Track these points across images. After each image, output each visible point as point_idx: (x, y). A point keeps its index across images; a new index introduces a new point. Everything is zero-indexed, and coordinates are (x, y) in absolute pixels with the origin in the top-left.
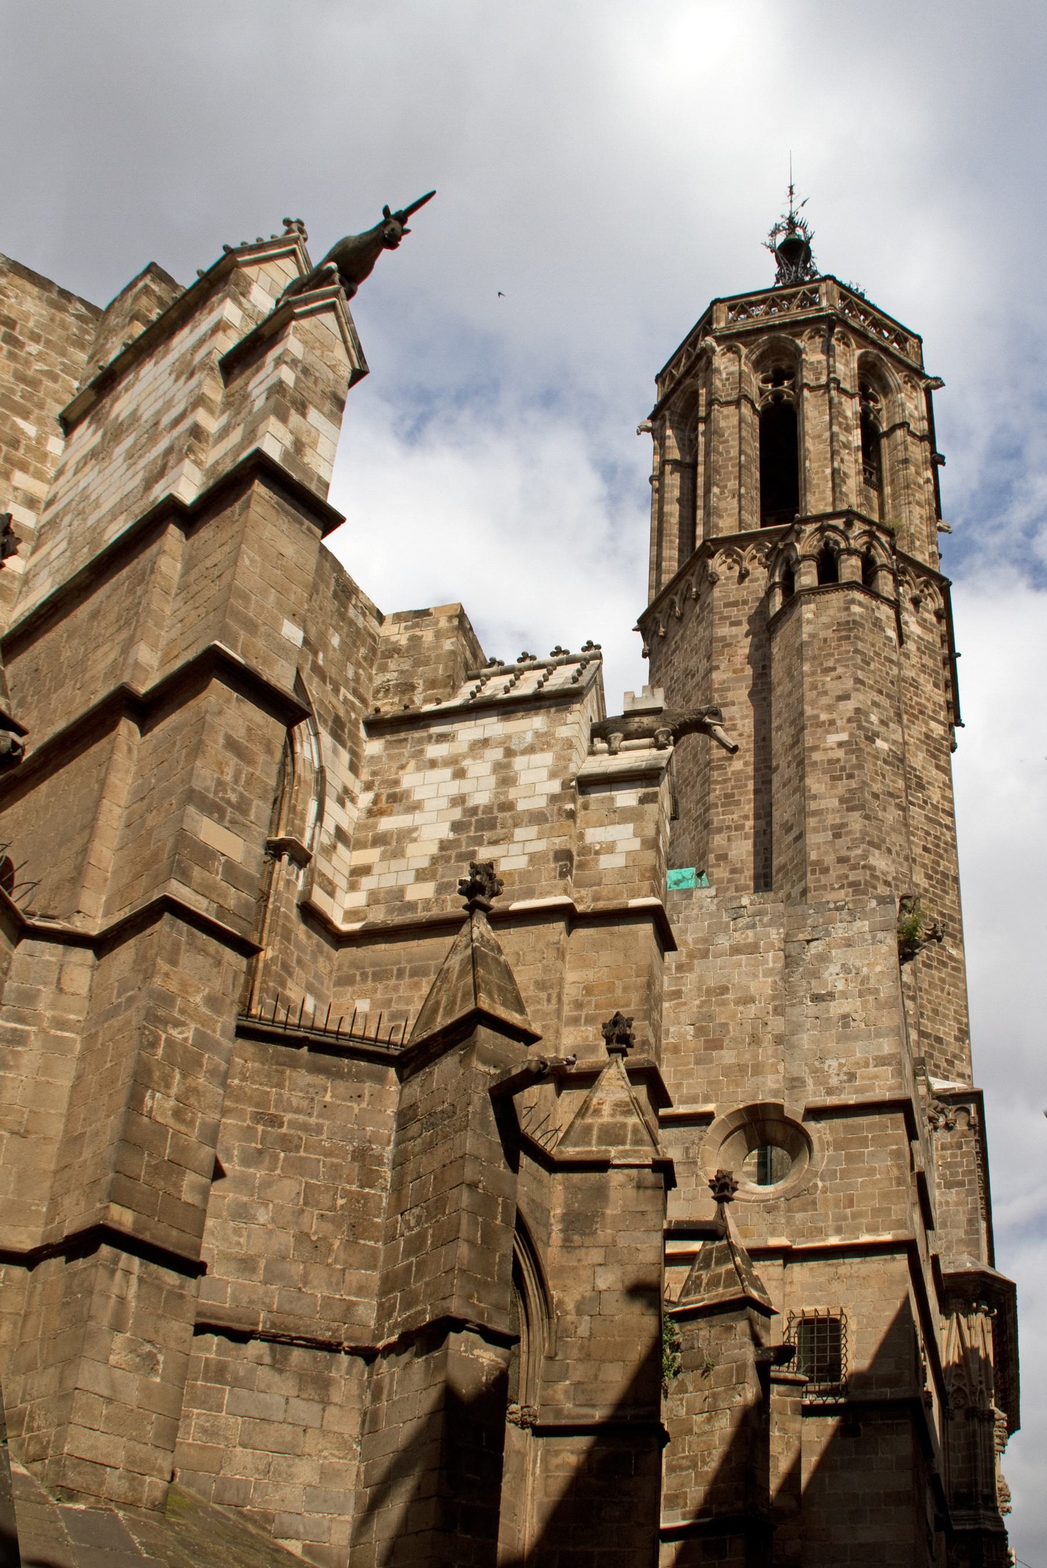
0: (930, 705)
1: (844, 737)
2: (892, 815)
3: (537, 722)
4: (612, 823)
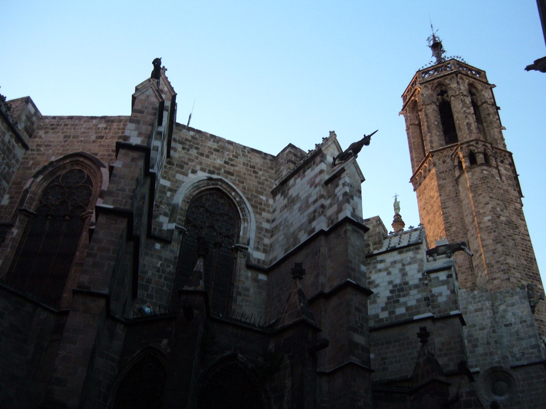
0: (514, 198)
1: (490, 218)
2: (511, 243)
3: (410, 254)
4: (440, 286)
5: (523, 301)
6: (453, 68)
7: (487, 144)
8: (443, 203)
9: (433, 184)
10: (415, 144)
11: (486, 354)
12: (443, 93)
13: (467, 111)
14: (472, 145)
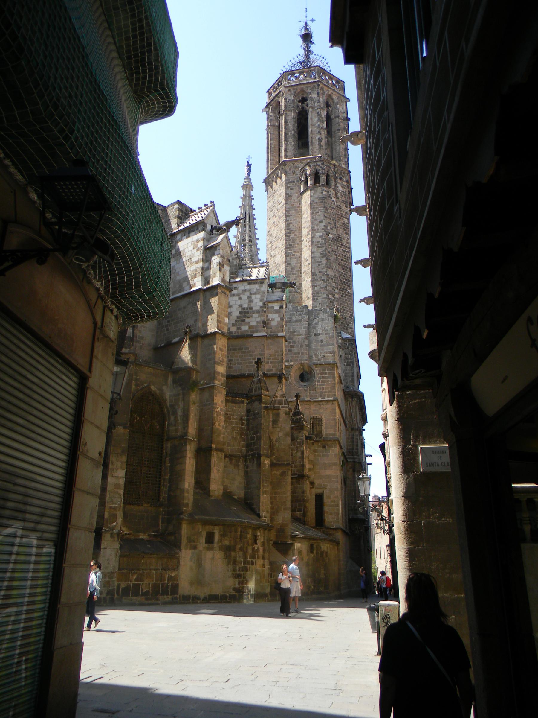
0: (344, 213)
1: (321, 234)
3: (257, 286)
4: (274, 313)
5: (330, 318)
6: (317, 76)
7: (331, 166)
8: (287, 211)
9: (282, 191)
10: (273, 146)
11: (299, 353)
12: (304, 100)
13: (321, 126)
14: (319, 165)
